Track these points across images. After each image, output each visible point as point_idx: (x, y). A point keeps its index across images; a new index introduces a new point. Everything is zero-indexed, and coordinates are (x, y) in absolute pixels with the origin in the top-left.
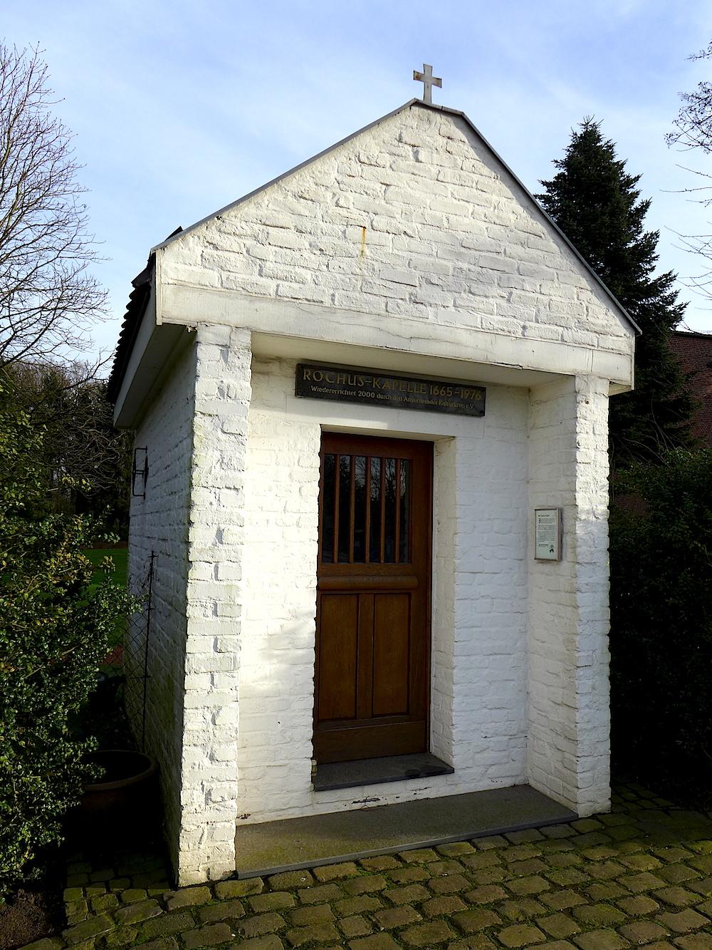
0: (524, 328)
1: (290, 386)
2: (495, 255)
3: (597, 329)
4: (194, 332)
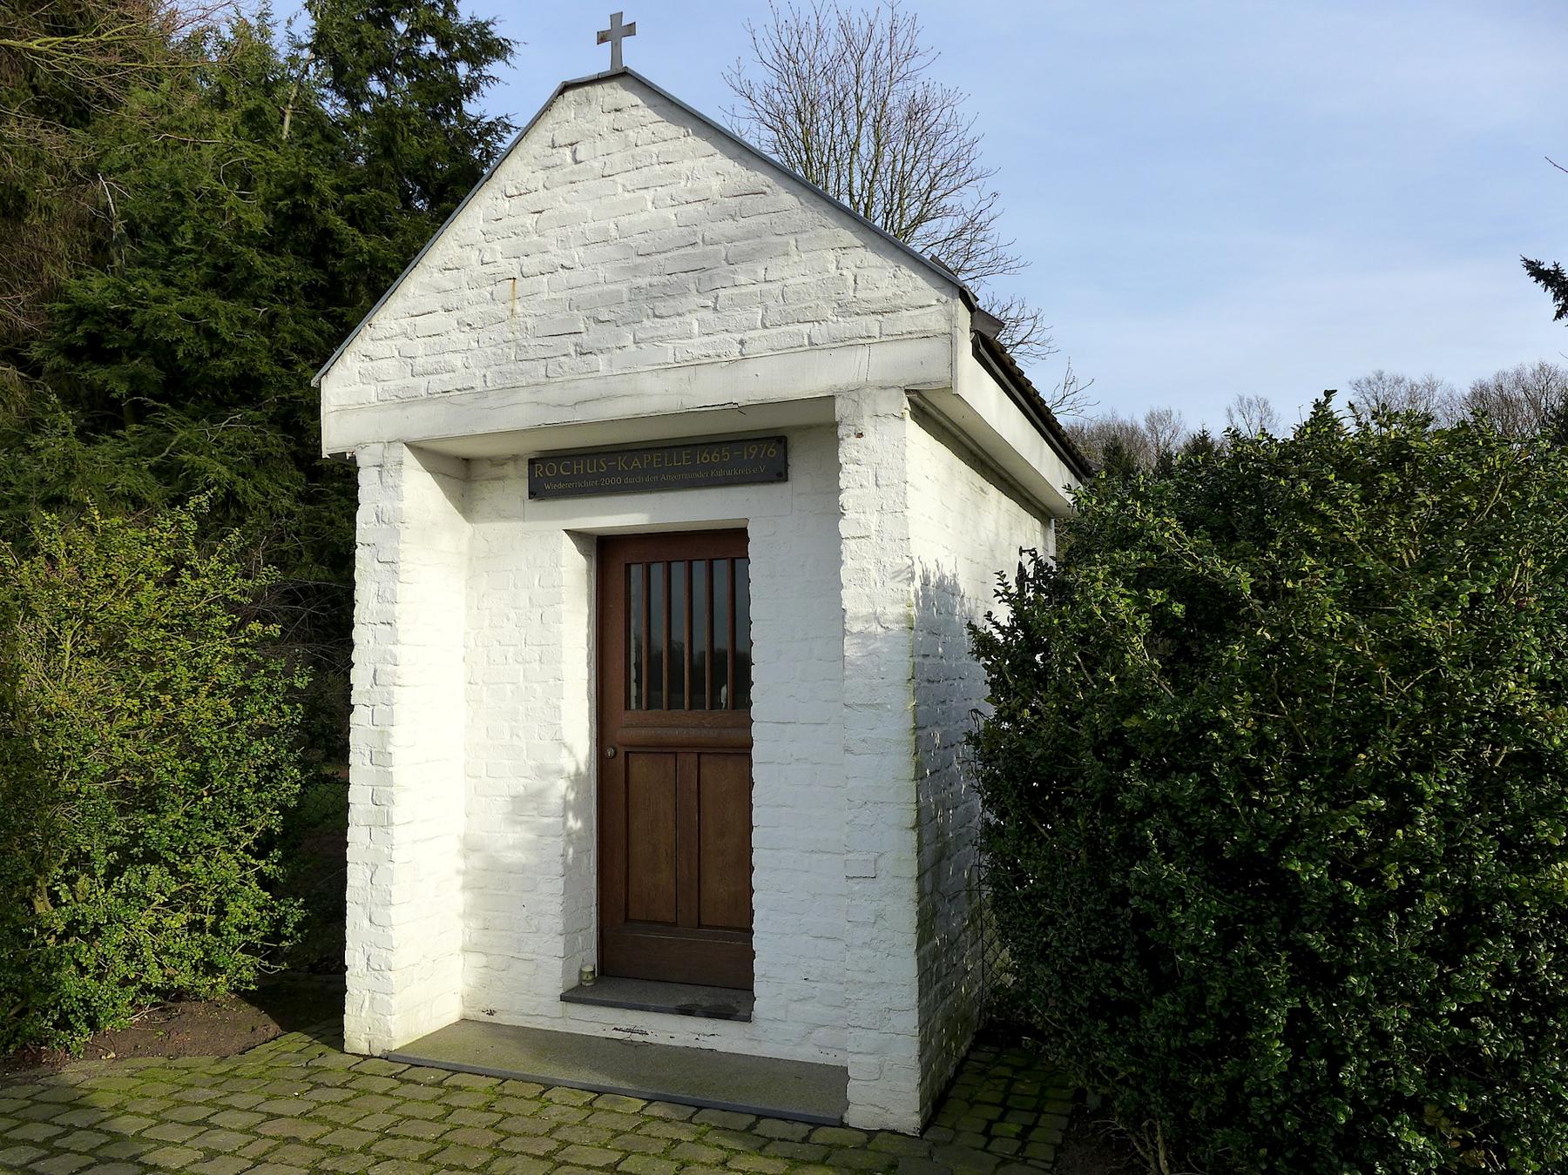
0: (742, 343)
1: (523, 487)
2: (690, 250)
3: (874, 307)
4: (353, 459)
